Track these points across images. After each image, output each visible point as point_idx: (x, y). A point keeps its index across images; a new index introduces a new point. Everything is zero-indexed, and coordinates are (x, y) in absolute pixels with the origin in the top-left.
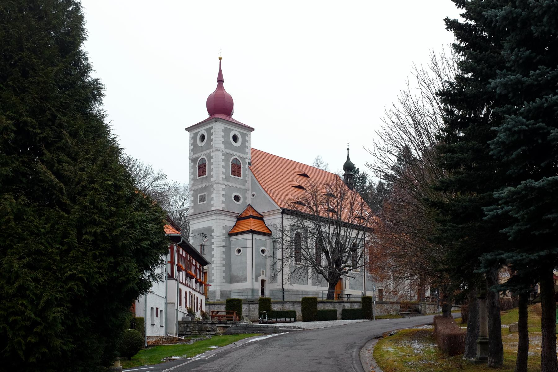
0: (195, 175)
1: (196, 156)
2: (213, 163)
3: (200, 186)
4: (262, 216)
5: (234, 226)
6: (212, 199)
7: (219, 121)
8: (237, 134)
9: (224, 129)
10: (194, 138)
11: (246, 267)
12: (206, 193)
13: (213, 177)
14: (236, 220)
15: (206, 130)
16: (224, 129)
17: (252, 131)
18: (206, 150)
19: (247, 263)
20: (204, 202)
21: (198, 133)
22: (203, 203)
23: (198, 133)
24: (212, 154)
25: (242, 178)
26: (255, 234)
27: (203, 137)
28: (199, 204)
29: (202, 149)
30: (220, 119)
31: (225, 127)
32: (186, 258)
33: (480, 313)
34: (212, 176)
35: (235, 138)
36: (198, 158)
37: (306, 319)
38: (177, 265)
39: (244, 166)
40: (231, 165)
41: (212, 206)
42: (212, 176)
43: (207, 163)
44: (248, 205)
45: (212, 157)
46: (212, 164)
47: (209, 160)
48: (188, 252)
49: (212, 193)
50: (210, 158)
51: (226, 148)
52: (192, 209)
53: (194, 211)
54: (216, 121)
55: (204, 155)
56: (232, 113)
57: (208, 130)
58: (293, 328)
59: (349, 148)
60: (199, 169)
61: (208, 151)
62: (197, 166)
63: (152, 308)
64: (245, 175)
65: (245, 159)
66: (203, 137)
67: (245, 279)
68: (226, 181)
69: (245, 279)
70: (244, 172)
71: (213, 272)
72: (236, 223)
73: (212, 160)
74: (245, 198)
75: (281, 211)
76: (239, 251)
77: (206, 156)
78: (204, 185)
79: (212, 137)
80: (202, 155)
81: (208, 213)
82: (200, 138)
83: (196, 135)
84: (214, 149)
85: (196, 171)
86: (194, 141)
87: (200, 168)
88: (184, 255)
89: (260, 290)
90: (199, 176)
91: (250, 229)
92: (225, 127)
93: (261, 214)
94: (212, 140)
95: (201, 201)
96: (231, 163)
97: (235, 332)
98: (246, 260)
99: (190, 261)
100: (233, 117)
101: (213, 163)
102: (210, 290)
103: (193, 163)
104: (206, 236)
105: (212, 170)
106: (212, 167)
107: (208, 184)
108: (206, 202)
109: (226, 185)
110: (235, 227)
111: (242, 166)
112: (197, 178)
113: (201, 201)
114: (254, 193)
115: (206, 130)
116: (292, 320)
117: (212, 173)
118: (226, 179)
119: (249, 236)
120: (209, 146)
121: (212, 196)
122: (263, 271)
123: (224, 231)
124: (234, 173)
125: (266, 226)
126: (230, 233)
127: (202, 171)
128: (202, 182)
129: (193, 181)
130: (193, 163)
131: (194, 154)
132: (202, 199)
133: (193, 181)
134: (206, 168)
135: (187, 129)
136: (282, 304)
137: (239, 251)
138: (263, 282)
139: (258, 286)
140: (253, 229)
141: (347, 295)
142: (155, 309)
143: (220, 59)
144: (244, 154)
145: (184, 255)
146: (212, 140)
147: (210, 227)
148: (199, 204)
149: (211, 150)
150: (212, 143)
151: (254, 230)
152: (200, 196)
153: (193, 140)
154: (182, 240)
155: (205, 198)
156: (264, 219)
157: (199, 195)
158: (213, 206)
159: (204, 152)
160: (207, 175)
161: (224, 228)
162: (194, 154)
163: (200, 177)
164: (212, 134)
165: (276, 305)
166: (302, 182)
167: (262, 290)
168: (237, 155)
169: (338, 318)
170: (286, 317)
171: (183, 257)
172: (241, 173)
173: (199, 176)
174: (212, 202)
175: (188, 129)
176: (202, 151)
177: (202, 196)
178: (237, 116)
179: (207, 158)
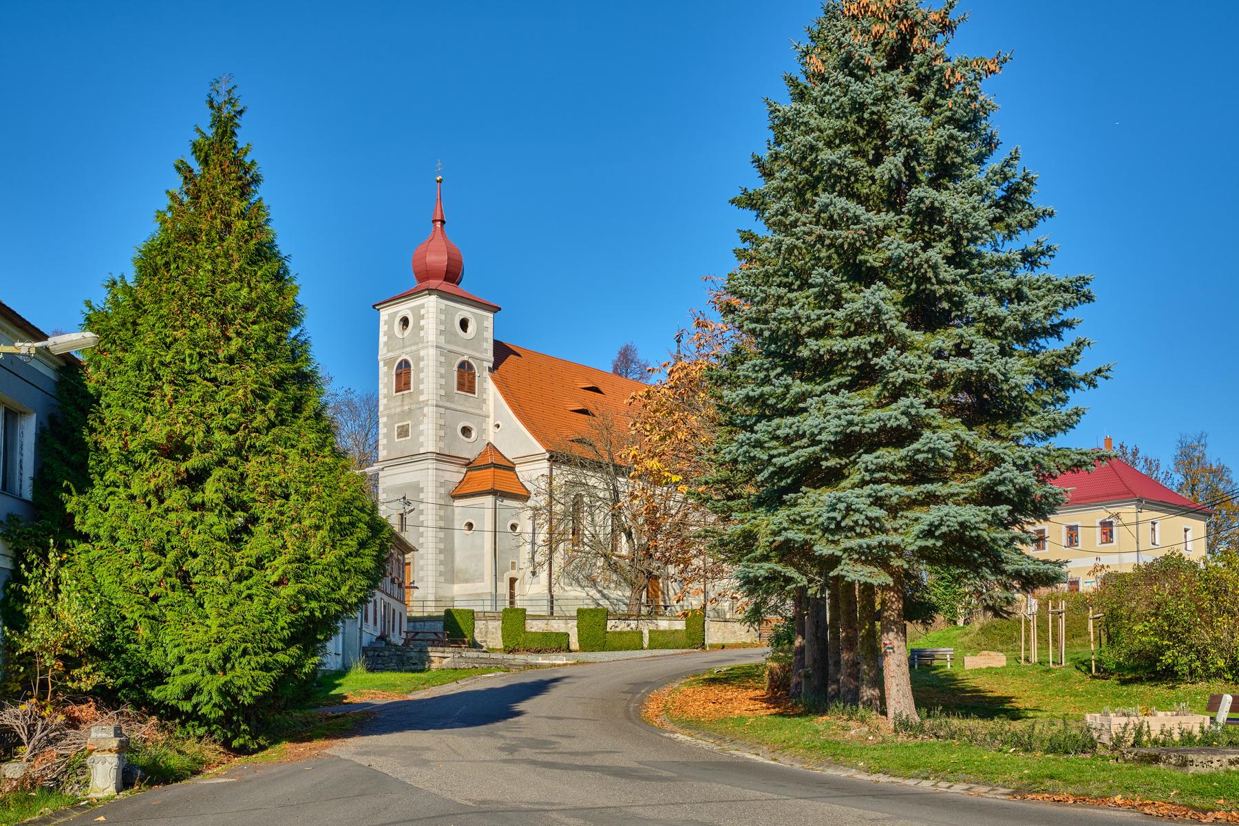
0: (389, 389)
1: (390, 355)
2: (423, 368)
6: (421, 433)
11: (482, 556)
12: (409, 422)
13: (422, 394)
15: (412, 309)
18: (410, 345)
21: (396, 313)
24: (422, 353)
25: (476, 396)
27: (405, 321)
33: (733, 664)
34: (421, 392)
35: (464, 324)
36: (395, 359)
37: (588, 644)
40: (456, 373)
41: (422, 445)
42: (421, 392)
43: (413, 367)
46: (422, 370)
47: (417, 364)
49: (422, 422)
50: (419, 359)
51: (448, 342)
57: (415, 310)
64: (484, 391)
66: (405, 321)
67: (481, 578)
69: (481, 578)
70: (481, 385)
71: (421, 562)
73: (422, 364)
74: (482, 431)
75: (547, 456)
79: (422, 323)
81: (414, 458)
84: (425, 344)
89: (508, 598)
94: (422, 328)
95: (400, 435)
96: (455, 368)
101: (423, 368)
106: (422, 375)
109: (446, 408)
111: (477, 374)
112: (394, 394)
113: (400, 435)
118: (448, 396)
119: (489, 500)
120: (417, 340)
121: (422, 427)
122: (513, 563)
123: (442, 491)
124: (461, 387)
131: (388, 351)
132: (403, 432)
137: (470, 526)
138: (513, 581)
139: (504, 588)
144: (481, 353)
146: (422, 328)
147: (418, 483)
148: (396, 440)
149: (420, 346)
150: (422, 333)
155: (407, 431)
159: (408, 350)
161: (442, 484)
162: (388, 351)
164: (422, 317)
165: (534, 622)
167: (512, 596)
169: (645, 646)
174: (422, 439)
177: (403, 426)
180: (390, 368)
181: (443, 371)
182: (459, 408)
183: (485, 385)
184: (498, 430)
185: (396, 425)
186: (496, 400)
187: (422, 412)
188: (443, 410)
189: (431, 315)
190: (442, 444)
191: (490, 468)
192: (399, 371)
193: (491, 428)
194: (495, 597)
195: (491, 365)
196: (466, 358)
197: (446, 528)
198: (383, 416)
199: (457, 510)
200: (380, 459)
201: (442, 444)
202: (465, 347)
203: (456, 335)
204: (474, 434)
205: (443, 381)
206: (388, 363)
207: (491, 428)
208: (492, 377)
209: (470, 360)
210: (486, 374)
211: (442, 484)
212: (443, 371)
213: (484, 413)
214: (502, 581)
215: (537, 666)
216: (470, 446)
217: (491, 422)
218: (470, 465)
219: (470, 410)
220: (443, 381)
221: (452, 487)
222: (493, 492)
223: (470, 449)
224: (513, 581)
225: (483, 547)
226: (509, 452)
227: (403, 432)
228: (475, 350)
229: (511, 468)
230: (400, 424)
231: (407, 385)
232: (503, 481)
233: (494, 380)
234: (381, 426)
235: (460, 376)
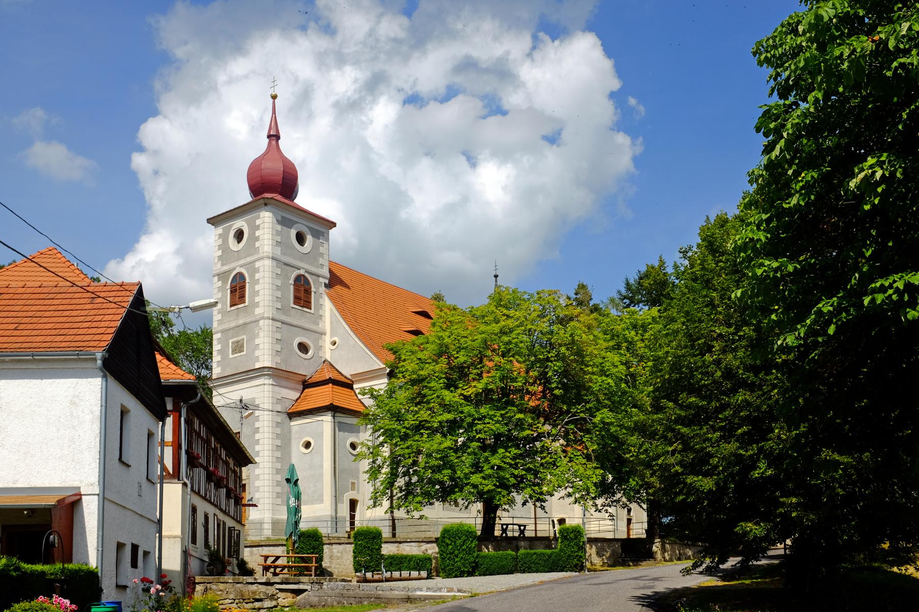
1: (226, 268)
3: (233, 324)
4: (353, 382)
5: (297, 399)
7: (270, 204)
8: (304, 230)
9: (280, 219)
10: (224, 237)
12: (245, 337)
13: (258, 306)
14: (301, 387)
16: (280, 219)
17: (331, 229)
18: (246, 257)
19: (323, 467)
20: (242, 354)
22: (239, 354)
23: (231, 226)
25: (312, 311)
26: (339, 412)
27: (239, 235)
28: (231, 356)
29: (238, 255)
30: (272, 201)
31: (282, 217)
32: (208, 442)
35: (301, 239)
36: (230, 271)
38: (187, 452)
39: (317, 288)
40: (292, 287)
41: (257, 359)
42: (257, 305)
43: (247, 280)
44: (324, 362)
45: (257, 270)
47: (252, 276)
48: (210, 430)
49: (257, 336)
51: (283, 254)
52: (218, 366)
53: (222, 370)
54: (266, 205)
55: (241, 266)
56: (294, 195)
58: (448, 592)
59: (498, 274)
60: (231, 292)
61: (249, 259)
62: (228, 286)
63: (120, 546)
64: (320, 306)
65: (318, 276)
66: (239, 235)
68: (284, 314)
70: (317, 300)
71: (257, 483)
72: (301, 394)
73: (257, 276)
76: (308, 445)
77: (246, 269)
78: (241, 322)
79: (257, 233)
80: (238, 267)
82: (235, 236)
83: (227, 232)
84: (260, 256)
85: (226, 298)
86: (223, 241)
87: (233, 291)
88: (203, 434)
90: (231, 306)
91: (329, 403)
92: (282, 217)
93: (350, 377)
94: (257, 239)
95: (234, 352)
96: (292, 281)
97: (319, 602)
98: (322, 461)
99: (215, 450)
100: (295, 201)
102: (251, 518)
103: (221, 282)
104: (248, 406)
105: (257, 293)
106: (257, 288)
107: (248, 320)
108: (245, 353)
109: (283, 323)
110: (299, 401)
111: (313, 289)
112: (229, 309)
113: (234, 352)
114: (335, 339)
115: (246, 221)
116: (424, 574)
117: (257, 299)
119: (327, 419)
120: (252, 249)
121: (257, 341)
122: (353, 484)
124: (297, 300)
125: (359, 400)
126: (290, 411)
127: (238, 296)
128: (237, 315)
129: (220, 315)
130: (221, 282)
131: (223, 265)
132: (238, 347)
133: (220, 315)
134: (245, 291)
135: (210, 221)
136: (396, 545)
138: (353, 504)
139: (344, 510)
140: (335, 404)
141: (520, 526)
142: (128, 550)
143: (274, 97)
144: (318, 267)
145: (203, 434)
146: (257, 239)
148: (231, 356)
149: (256, 257)
150: (257, 244)
151: (338, 404)
152: (233, 343)
153: (221, 240)
154: (199, 395)
155: (242, 346)
156: (355, 386)
157: (231, 341)
158: (258, 361)
159: (242, 262)
160: (247, 304)
161: (279, 401)
162: (223, 265)
163: (233, 308)
164: (258, 228)
166: (422, 323)
167: (352, 517)
168: (304, 267)
170: (410, 569)
171: (202, 439)
172: (310, 303)
173: (231, 306)
174: (257, 353)
175: (211, 221)
176: (238, 260)
177: (238, 342)
178: (303, 199)
179: (248, 272)
180: (225, 283)
181: (279, 283)
182: (295, 322)
183: (321, 301)
184: (333, 347)
185: (231, 341)
186: (332, 315)
187: (258, 325)
188: (279, 324)
189: (266, 225)
190: (278, 359)
191: (327, 384)
192: (234, 284)
193: (328, 346)
194: (336, 520)
195: (327, 282)
196: (302, 272)
197: (283, 446)
198: (217, 333)
199: (294, 429)
200: (214, 377)
201: (278, 359)
202: (301, 260)
203: (293, 248)
204: (310, 353)
205: (279, 294)
206: (222, 276)
207: (328, 346)
208: (327, 294)
209: (307, 275)
210: (322, 289)
211: (279, 401)
212: (279, 283)
213: (319, 330)
214: (342, 503)
215: (428, 589)
216: (307, 362)
217: (328, 339)
218: (307, 385)
219: (306, 325)
220: (279, 294)
221: (288, 404)
222: (333, 409)
223: (306, 367)
224: (353, 504)
225: (322, 466)
226: (347, 371)
227: (238, 347)
228: (310, 264)
229: (349, 386)
230: (235, 339)
231: (242, 297)
232: (341, 397)
233: (331, 298)
234: (215, 342)
235: (296, 290)
